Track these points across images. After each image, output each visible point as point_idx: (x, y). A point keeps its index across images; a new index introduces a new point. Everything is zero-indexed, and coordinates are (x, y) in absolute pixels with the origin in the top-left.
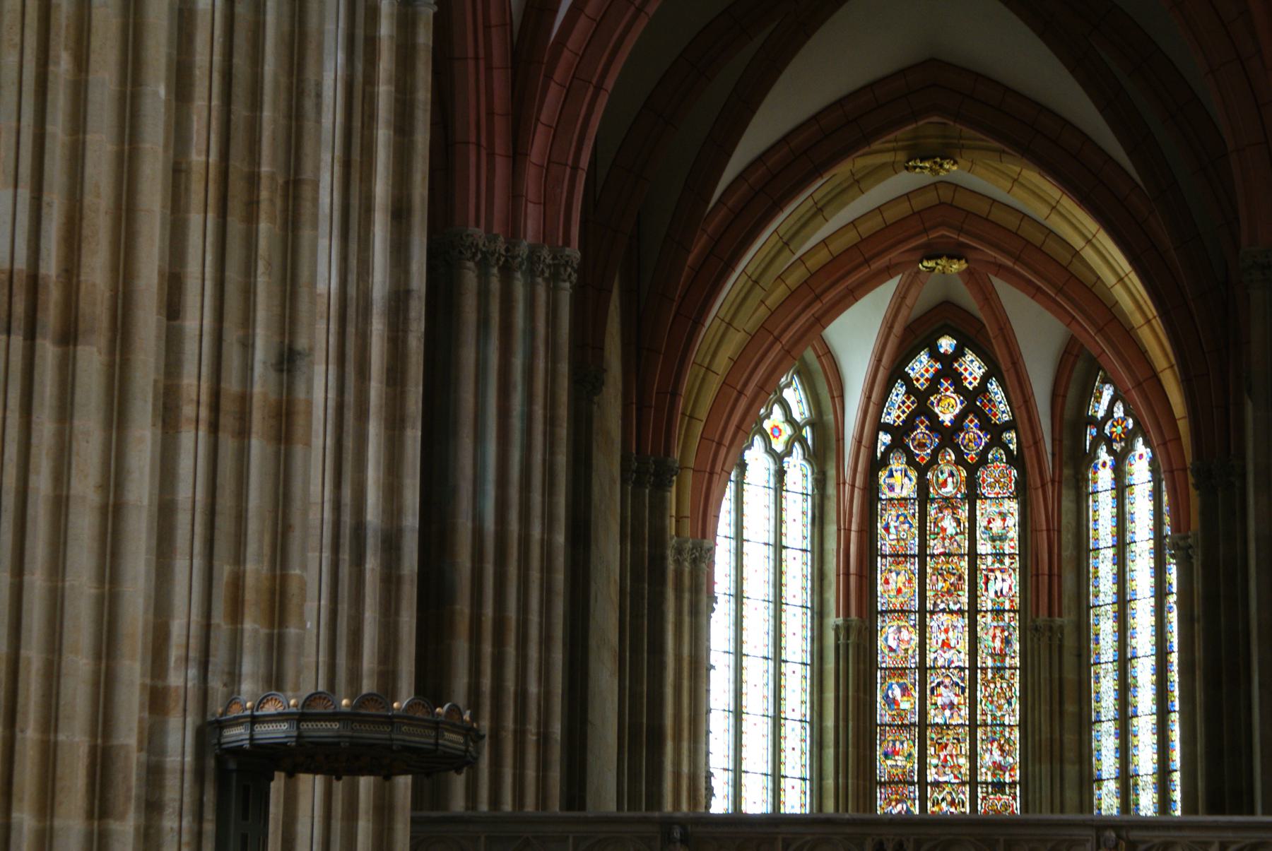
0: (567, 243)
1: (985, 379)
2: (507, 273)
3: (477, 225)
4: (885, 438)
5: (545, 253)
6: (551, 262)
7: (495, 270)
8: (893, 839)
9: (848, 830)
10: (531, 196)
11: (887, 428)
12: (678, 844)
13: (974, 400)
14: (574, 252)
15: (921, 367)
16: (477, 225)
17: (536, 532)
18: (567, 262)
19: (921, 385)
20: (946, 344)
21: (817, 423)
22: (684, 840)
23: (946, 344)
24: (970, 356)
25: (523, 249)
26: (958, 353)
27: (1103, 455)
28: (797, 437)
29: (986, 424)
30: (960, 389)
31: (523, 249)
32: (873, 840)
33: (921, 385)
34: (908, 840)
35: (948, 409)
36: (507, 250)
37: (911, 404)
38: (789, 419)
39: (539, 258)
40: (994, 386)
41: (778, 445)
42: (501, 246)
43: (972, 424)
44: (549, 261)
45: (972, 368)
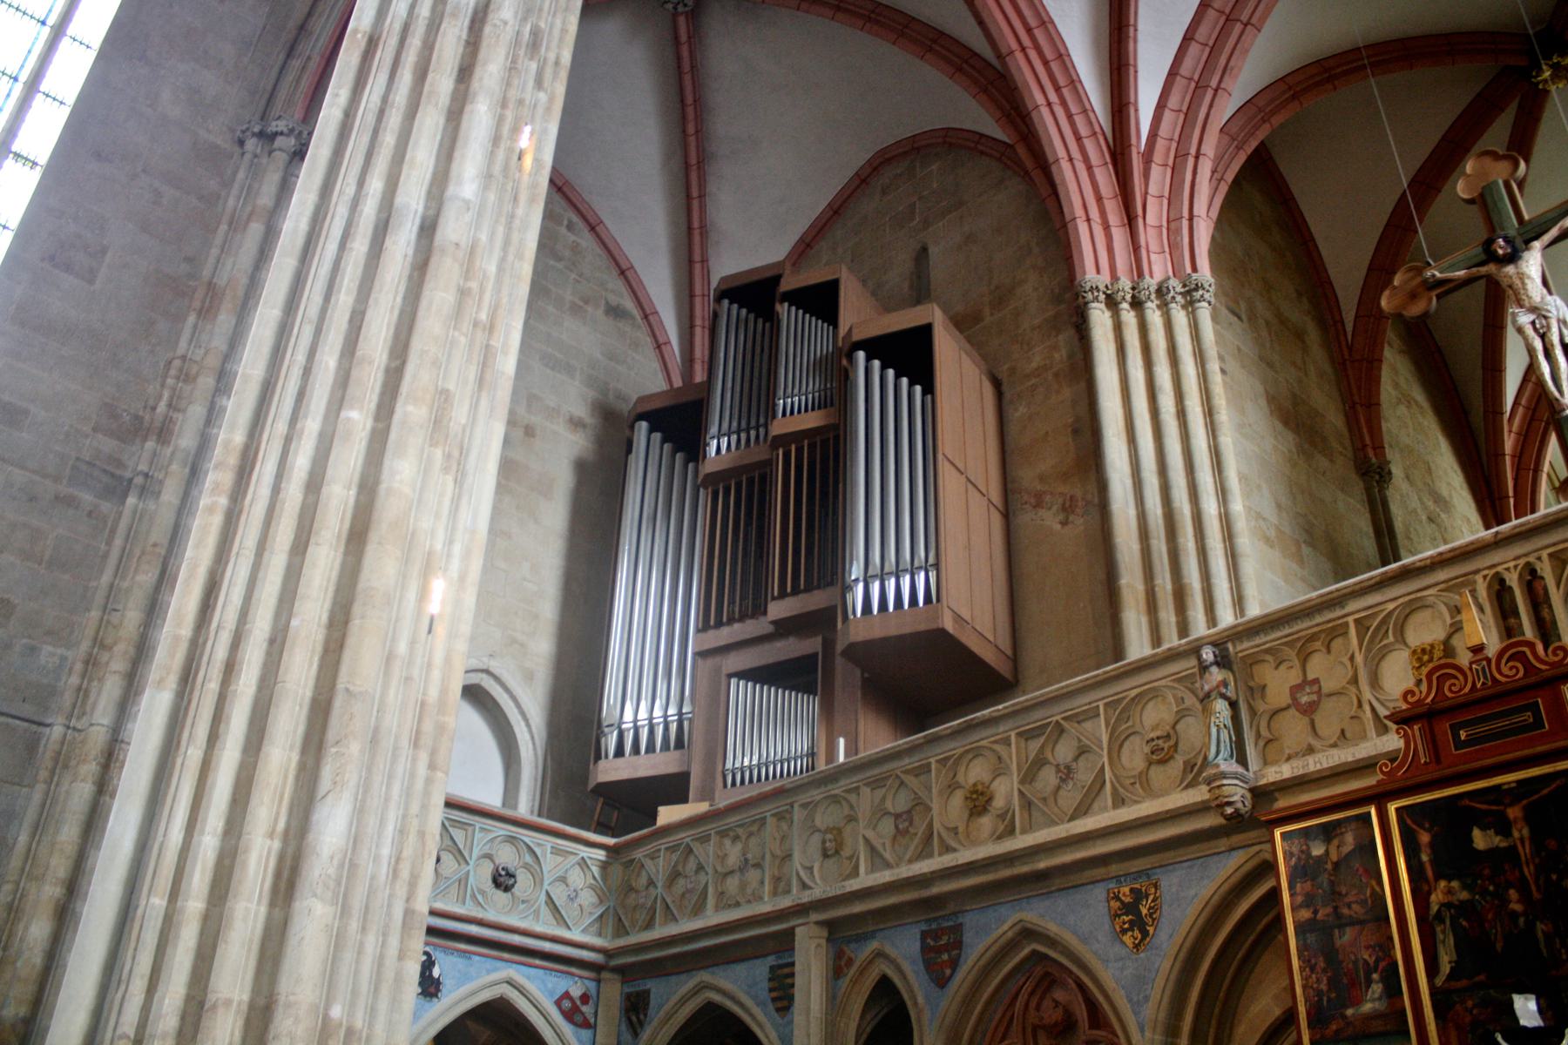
0: (1195, 269)
2: (1137, 304)
3: (1098, 272)
5: (1174, 283)
6: (1182, 290)
7: (1125, 305)
8: (1516, 567)
9: (1442, 575)
10: (1154, 247)
12: (1214, 669)
14: (1205, 273)
16: (1098, 272)
17: (1210, 507)
18: (1197, 285)
22: (1223, 661)
25: (1151, 283)
31: (1151, 283)
32: (1485, 577)
34: (1539, 559)
36: (1133, 289)
39: (1168, 288)
42: (1125, 283)
44: (1179, 289)
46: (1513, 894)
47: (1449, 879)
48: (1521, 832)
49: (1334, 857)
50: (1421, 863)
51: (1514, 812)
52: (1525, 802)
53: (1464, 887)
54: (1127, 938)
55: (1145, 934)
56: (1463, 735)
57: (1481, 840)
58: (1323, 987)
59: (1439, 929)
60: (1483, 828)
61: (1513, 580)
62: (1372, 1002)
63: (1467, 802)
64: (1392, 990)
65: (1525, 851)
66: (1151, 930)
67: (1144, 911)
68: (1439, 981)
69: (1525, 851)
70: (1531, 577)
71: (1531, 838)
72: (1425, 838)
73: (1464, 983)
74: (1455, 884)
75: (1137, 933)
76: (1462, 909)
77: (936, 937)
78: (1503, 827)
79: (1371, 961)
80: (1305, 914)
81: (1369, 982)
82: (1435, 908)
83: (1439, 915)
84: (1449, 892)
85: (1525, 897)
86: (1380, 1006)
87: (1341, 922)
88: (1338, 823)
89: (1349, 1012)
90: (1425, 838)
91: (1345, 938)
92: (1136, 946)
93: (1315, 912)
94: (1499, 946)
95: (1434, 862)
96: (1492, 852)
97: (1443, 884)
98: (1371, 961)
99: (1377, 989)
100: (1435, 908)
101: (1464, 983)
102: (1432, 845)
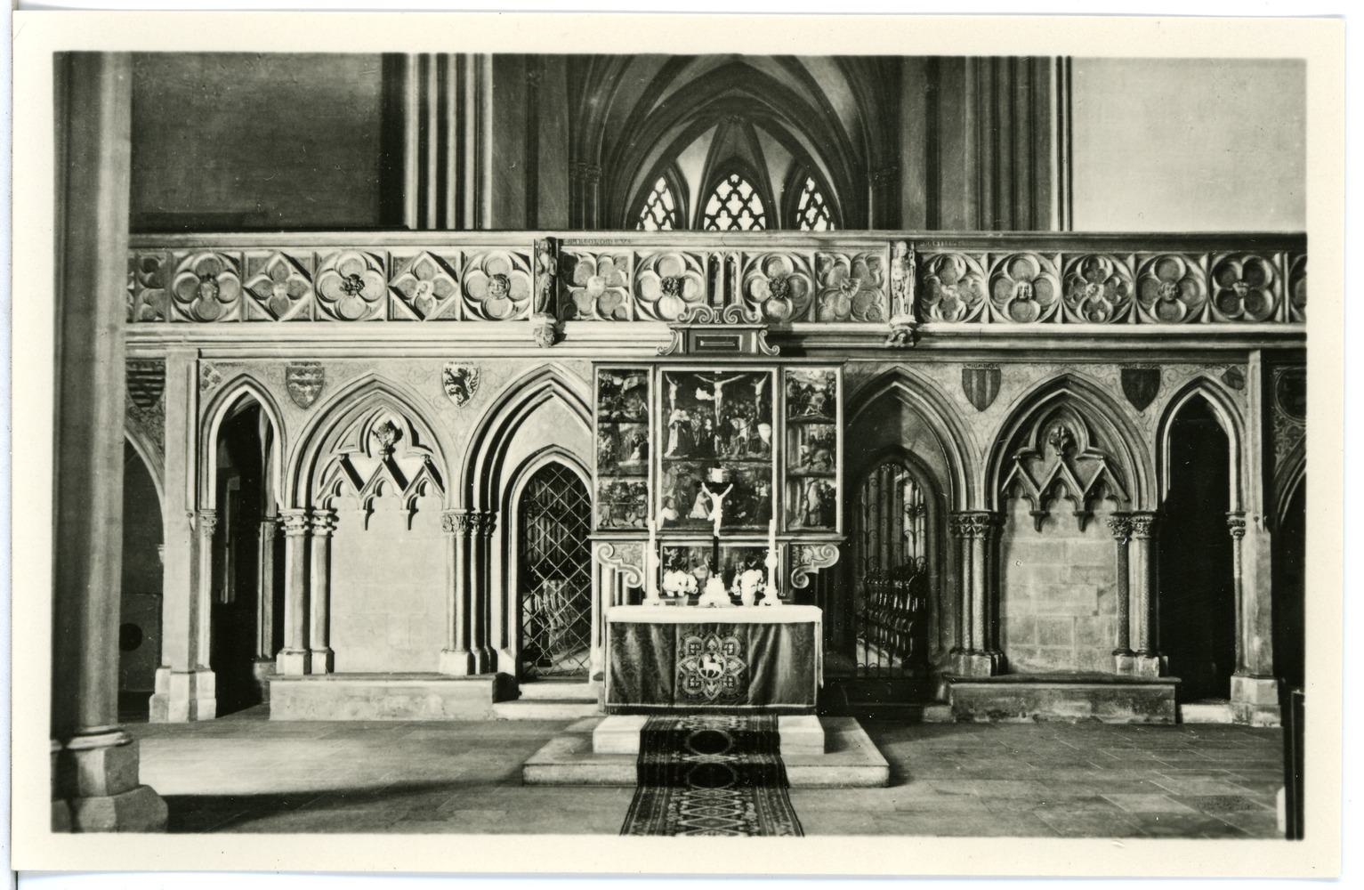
1: (751, 195)
4: (707, 222)
11: (709, 216)
13: (746, 203)
15: (724, 189)
19: (724, 197)
20: (735, 178)
21: (677, 210)
23: (735, 178)
24: (744, 182)
26: (739, 183)
27: (804, 223)
28: (667, 217)
29: (752, 215)
30: (740, 198)
33: (724, 197)
35: (735, 205)
37: (719, 205)
38: (664, 208)
40: (755, 197)
41: (660, 220)
43: (746, 213)
45: (745, 189)
46: (709, 422)
47: (681, 409)
48: (718, 395)
49: (626, 387)
50: (669, 400)
51: (718, 385)
52: (724, 382)
53: (688, 414)
54: (454, 398)
55: (466, 397)
56: (702, 343)
57: (701, 395)
58: (609, 450)
59: (672, 431)
60: (702, 389)
61: (721, 260)
62: (633, 460)
63: (697, 375)
64: (644, 455)
65: (718, 404)
66: (471, 395)
67: (467, 384)
68: (667, 455)
69: (718, 404)
70: (728, 264)
71: (723, 398)
72: (673, 388)
73: (678, 457)
74: (684, 412)
75: (461, 396)
76: (685, 425)
77: (301, 373)
78: (711, 391)
79: (636, 441)
80: (605, 413)
81: (633, 451)
82: (671, 423)
83: (673, 426)
84: (681, 416)
85: (713, 424)
86: (637, 463)
87: (623, 419)
88: (629, 371)
89: (621, 464)
90: (673, 388)
91: (623, 427)
92: (460, 404)
93: (611, 413)
94: (697, 443)
95: (676, 400)
96: (704, 402)
97: (678, 411)
98: (636, 441)
99: (637, 454)
100: (671, 423)
101: (678, 457)
102: (678, 393)
